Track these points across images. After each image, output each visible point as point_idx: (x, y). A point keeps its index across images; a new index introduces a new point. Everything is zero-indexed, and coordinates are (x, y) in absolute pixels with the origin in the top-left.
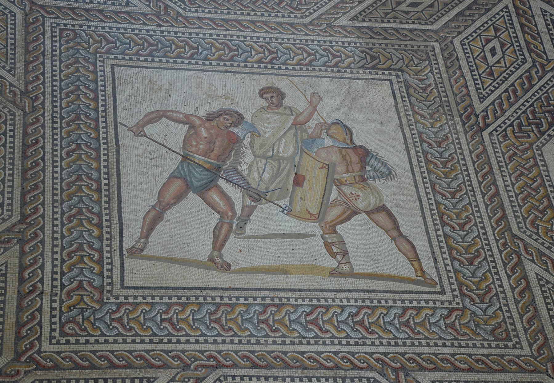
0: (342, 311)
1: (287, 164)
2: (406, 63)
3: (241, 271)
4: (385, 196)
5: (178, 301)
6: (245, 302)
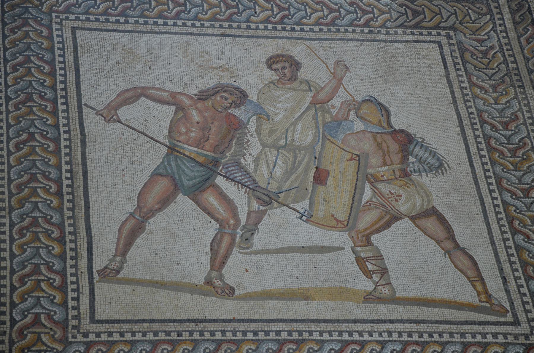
0: (382, 348)
1: (305, 155)
2: (460, 19)
3: (248, 297)
4: (434, 195)
5: (166, 338)
6: (254, 338)
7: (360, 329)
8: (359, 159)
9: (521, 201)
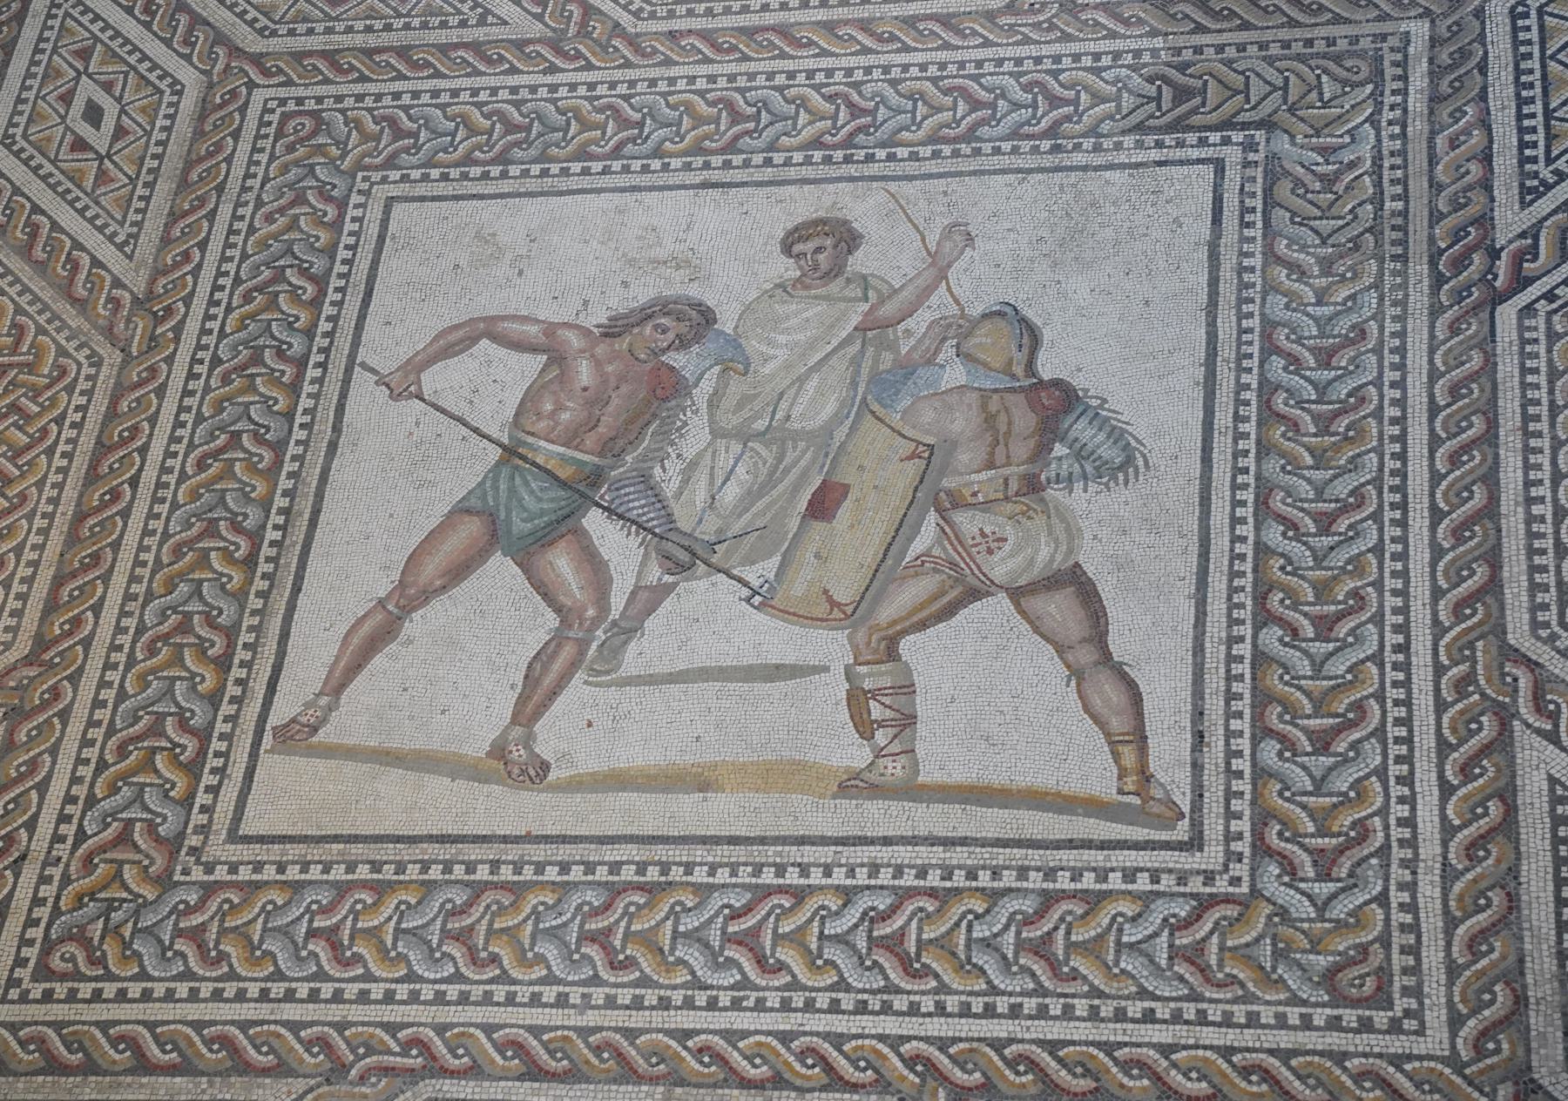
0: (845, 905)
1: (804, 452)
4: (1087, 535)
7: (806, 860)
8: (931, 454)
9: (1305, 544)
